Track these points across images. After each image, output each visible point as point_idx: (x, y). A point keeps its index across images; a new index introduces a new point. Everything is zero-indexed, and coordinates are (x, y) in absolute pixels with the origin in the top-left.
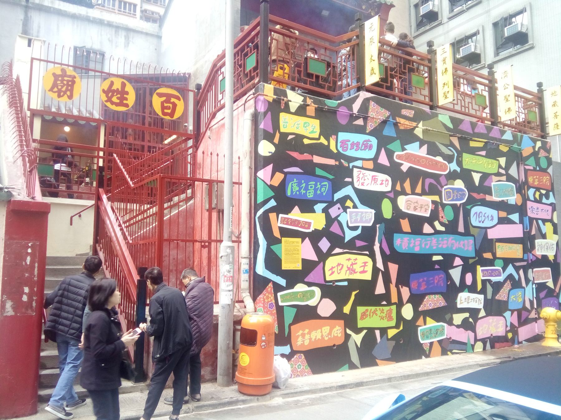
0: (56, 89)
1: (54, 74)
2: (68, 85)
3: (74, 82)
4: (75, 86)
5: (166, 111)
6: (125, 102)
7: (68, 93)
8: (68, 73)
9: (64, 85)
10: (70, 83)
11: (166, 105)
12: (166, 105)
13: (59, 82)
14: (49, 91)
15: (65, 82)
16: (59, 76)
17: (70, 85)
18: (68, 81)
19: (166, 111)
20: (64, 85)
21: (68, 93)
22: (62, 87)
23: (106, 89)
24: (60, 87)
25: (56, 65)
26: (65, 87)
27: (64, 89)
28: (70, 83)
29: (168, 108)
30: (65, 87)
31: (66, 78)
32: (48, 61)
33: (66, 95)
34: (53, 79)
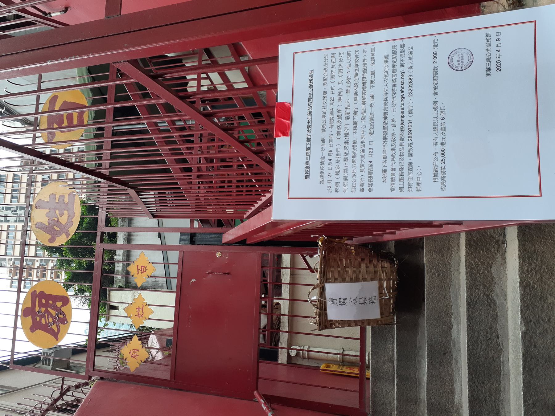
0: (54, 327)
1: (33, 329)
2: (46, 305)
3: (42, 295)
4: (47, 292)
5: (75, 122)
6: (66, 200)
7: (59, 304)
8: (29, 305)
9: (47, 311)
10: (44, 301)
11: (66, 124)
12: (66, 124)
13: (43, 322)
14: (57, 339)
15: (43, 309)
16: (33, 319)
17: (47, 302)
18: (41, 305)
19: (75, 122)
20: (47, 311)
21: (59, 304)
22: (50, 315)
23: (50, 237)
24: (51, 320)
25: (19, 324)
26: (49, 309)
27: (53, 312)
28: (44, 301)
29: (70, 117)
30: (49, 309)
31: (37, 309)
32: (14, 340)
33: (62, 309)
34: (38, 331)
